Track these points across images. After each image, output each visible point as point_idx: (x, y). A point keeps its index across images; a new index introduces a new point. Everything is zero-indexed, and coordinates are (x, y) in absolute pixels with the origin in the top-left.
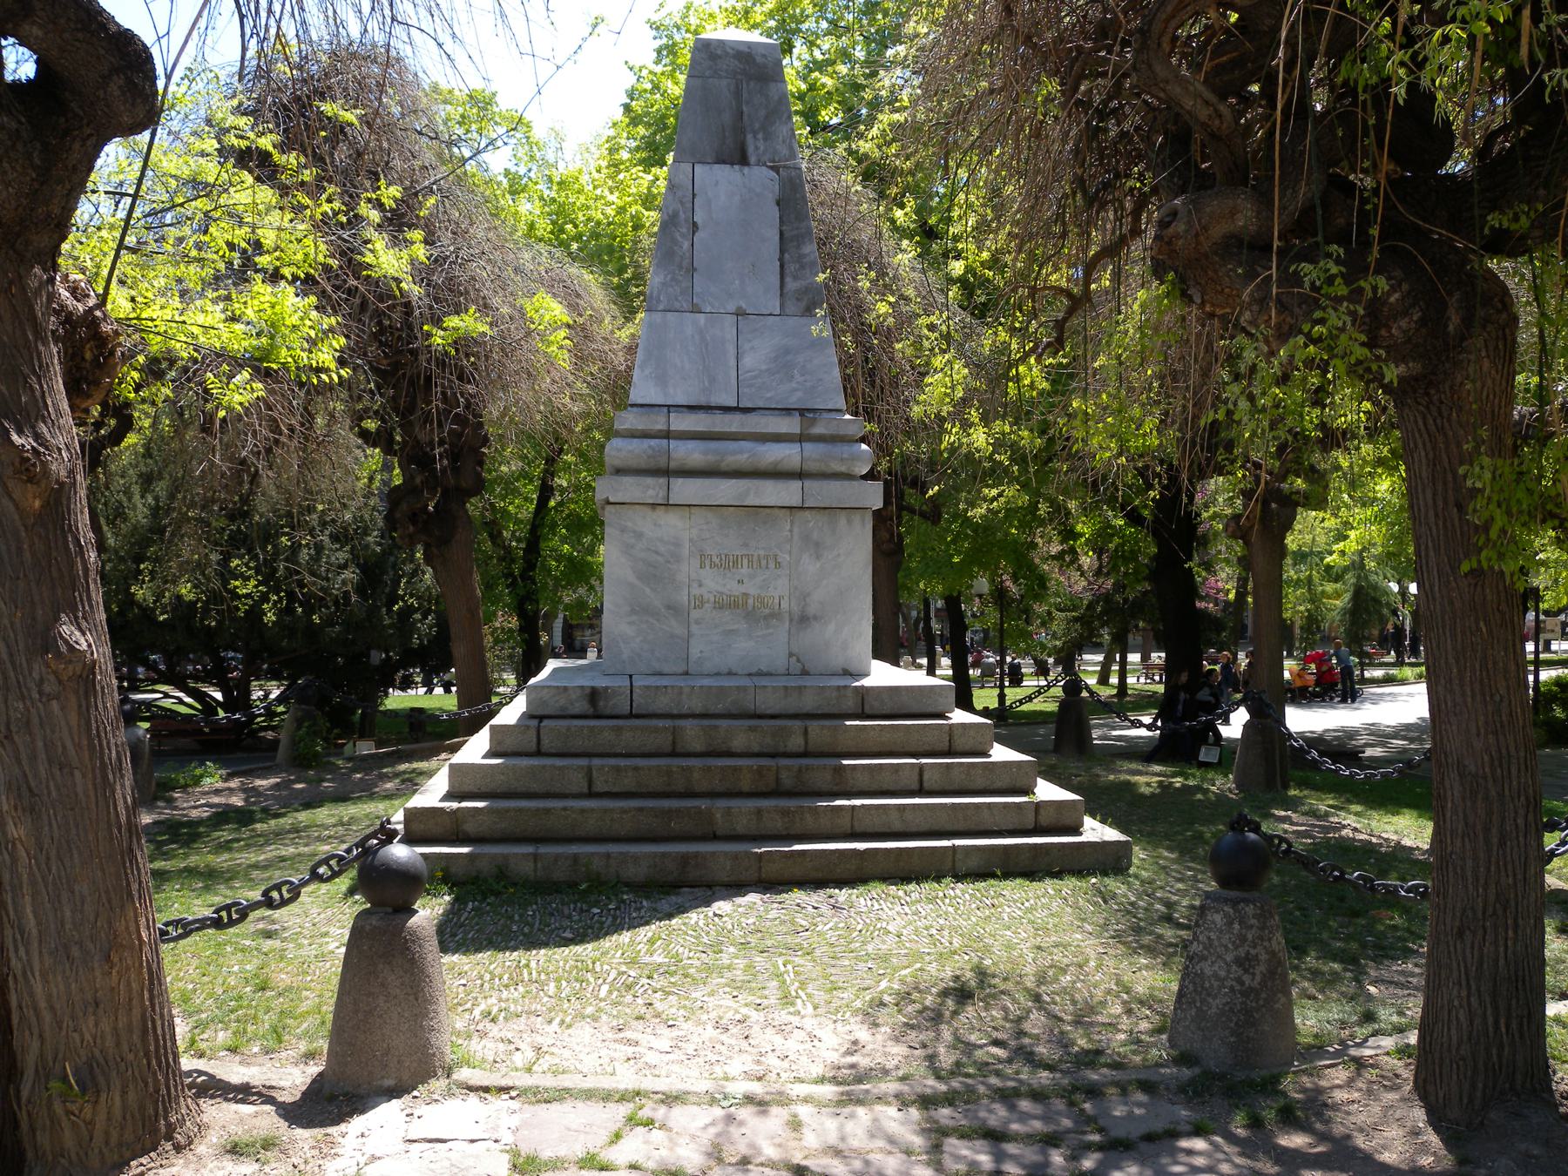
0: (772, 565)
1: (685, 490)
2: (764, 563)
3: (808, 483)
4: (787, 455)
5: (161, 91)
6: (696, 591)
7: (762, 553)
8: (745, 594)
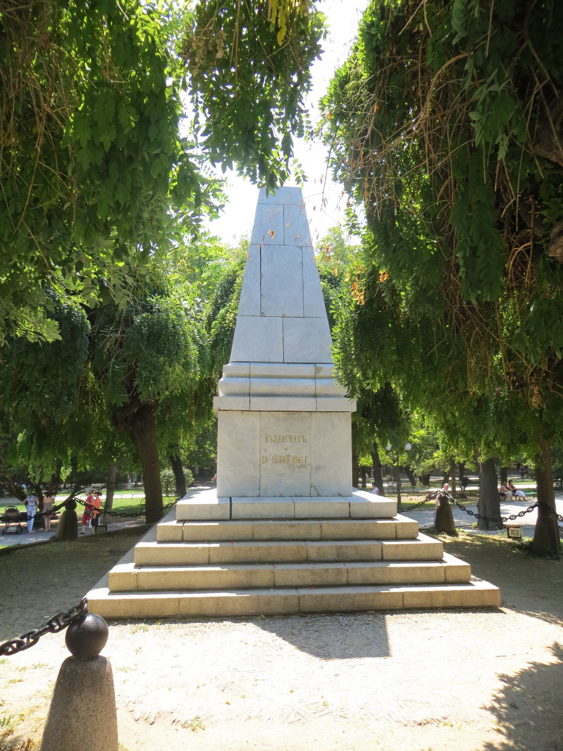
0: (301, 440)
1: (258, 403)
2: (297, 439)
3: (319, 400)
4: (309, 386)
5: (200, 111)
6: (263, 454)
7: (296, 434)
8: (289, 456)
